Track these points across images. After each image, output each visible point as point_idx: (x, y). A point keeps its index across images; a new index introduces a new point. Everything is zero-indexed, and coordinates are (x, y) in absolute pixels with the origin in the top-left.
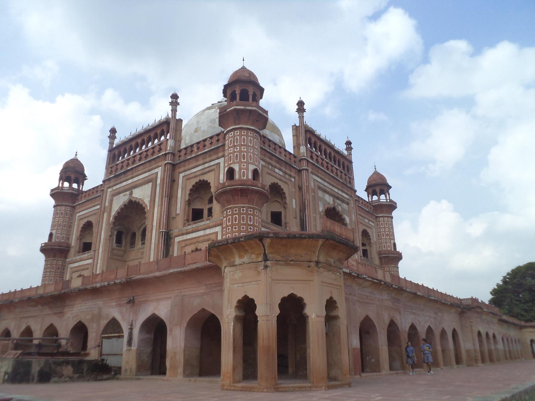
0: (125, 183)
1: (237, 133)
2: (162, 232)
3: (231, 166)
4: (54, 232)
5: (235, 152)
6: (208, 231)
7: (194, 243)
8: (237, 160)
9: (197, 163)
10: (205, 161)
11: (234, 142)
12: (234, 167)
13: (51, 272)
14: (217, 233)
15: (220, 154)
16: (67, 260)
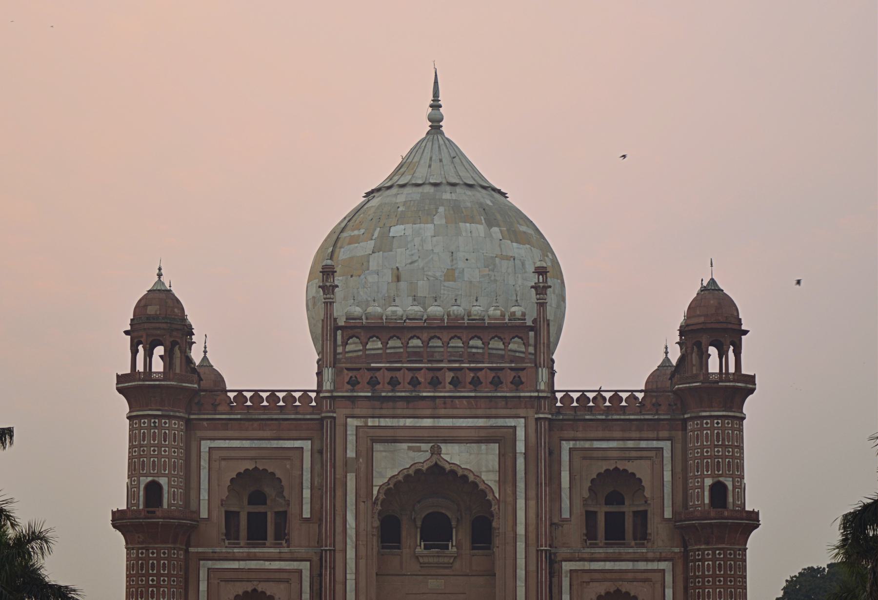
0: (409, 422)
1: (728, 423)
2: (546, 551)
3: (721, 479)
4: (163, 481)
5: (727, 457)
6: (642, 565)
7: (611, 580)
8: (729, 471)
9: (607, 434)
10: (627, 435)
11: (723, 440)
12: (727, 483)
13: (173, 576)
14: (664, 570)
15: (662, 434)
16: (191, 550)
